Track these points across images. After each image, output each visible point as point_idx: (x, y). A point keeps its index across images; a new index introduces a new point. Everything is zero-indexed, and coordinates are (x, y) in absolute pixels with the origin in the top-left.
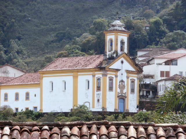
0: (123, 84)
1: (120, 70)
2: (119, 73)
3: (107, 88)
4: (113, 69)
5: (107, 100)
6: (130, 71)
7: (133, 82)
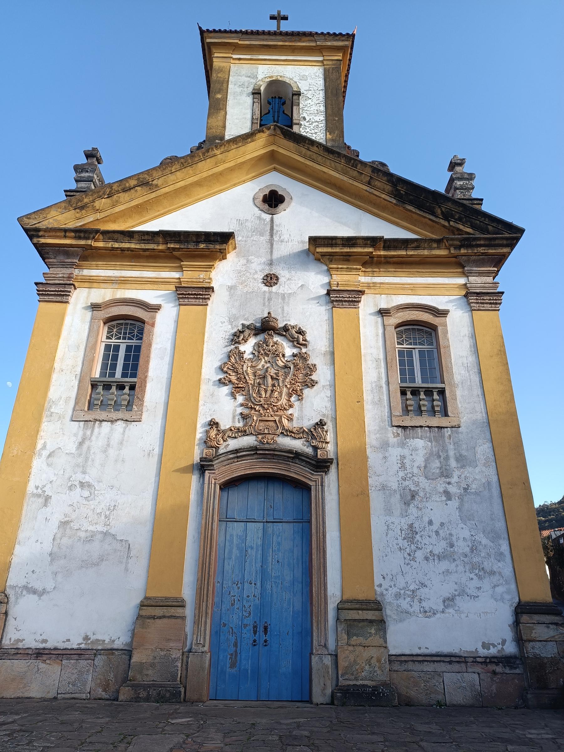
0: (289, 350)
1: (225, 238)
2: (222, 274)
3: (54, 393)
4: (130, 235)
5: (30, 507)
6: (350, 241)
7: (419, 331)
